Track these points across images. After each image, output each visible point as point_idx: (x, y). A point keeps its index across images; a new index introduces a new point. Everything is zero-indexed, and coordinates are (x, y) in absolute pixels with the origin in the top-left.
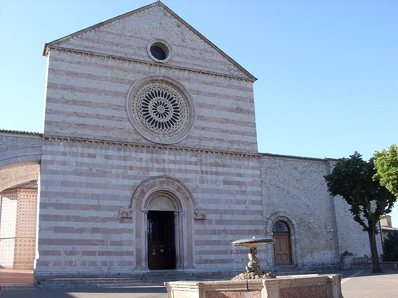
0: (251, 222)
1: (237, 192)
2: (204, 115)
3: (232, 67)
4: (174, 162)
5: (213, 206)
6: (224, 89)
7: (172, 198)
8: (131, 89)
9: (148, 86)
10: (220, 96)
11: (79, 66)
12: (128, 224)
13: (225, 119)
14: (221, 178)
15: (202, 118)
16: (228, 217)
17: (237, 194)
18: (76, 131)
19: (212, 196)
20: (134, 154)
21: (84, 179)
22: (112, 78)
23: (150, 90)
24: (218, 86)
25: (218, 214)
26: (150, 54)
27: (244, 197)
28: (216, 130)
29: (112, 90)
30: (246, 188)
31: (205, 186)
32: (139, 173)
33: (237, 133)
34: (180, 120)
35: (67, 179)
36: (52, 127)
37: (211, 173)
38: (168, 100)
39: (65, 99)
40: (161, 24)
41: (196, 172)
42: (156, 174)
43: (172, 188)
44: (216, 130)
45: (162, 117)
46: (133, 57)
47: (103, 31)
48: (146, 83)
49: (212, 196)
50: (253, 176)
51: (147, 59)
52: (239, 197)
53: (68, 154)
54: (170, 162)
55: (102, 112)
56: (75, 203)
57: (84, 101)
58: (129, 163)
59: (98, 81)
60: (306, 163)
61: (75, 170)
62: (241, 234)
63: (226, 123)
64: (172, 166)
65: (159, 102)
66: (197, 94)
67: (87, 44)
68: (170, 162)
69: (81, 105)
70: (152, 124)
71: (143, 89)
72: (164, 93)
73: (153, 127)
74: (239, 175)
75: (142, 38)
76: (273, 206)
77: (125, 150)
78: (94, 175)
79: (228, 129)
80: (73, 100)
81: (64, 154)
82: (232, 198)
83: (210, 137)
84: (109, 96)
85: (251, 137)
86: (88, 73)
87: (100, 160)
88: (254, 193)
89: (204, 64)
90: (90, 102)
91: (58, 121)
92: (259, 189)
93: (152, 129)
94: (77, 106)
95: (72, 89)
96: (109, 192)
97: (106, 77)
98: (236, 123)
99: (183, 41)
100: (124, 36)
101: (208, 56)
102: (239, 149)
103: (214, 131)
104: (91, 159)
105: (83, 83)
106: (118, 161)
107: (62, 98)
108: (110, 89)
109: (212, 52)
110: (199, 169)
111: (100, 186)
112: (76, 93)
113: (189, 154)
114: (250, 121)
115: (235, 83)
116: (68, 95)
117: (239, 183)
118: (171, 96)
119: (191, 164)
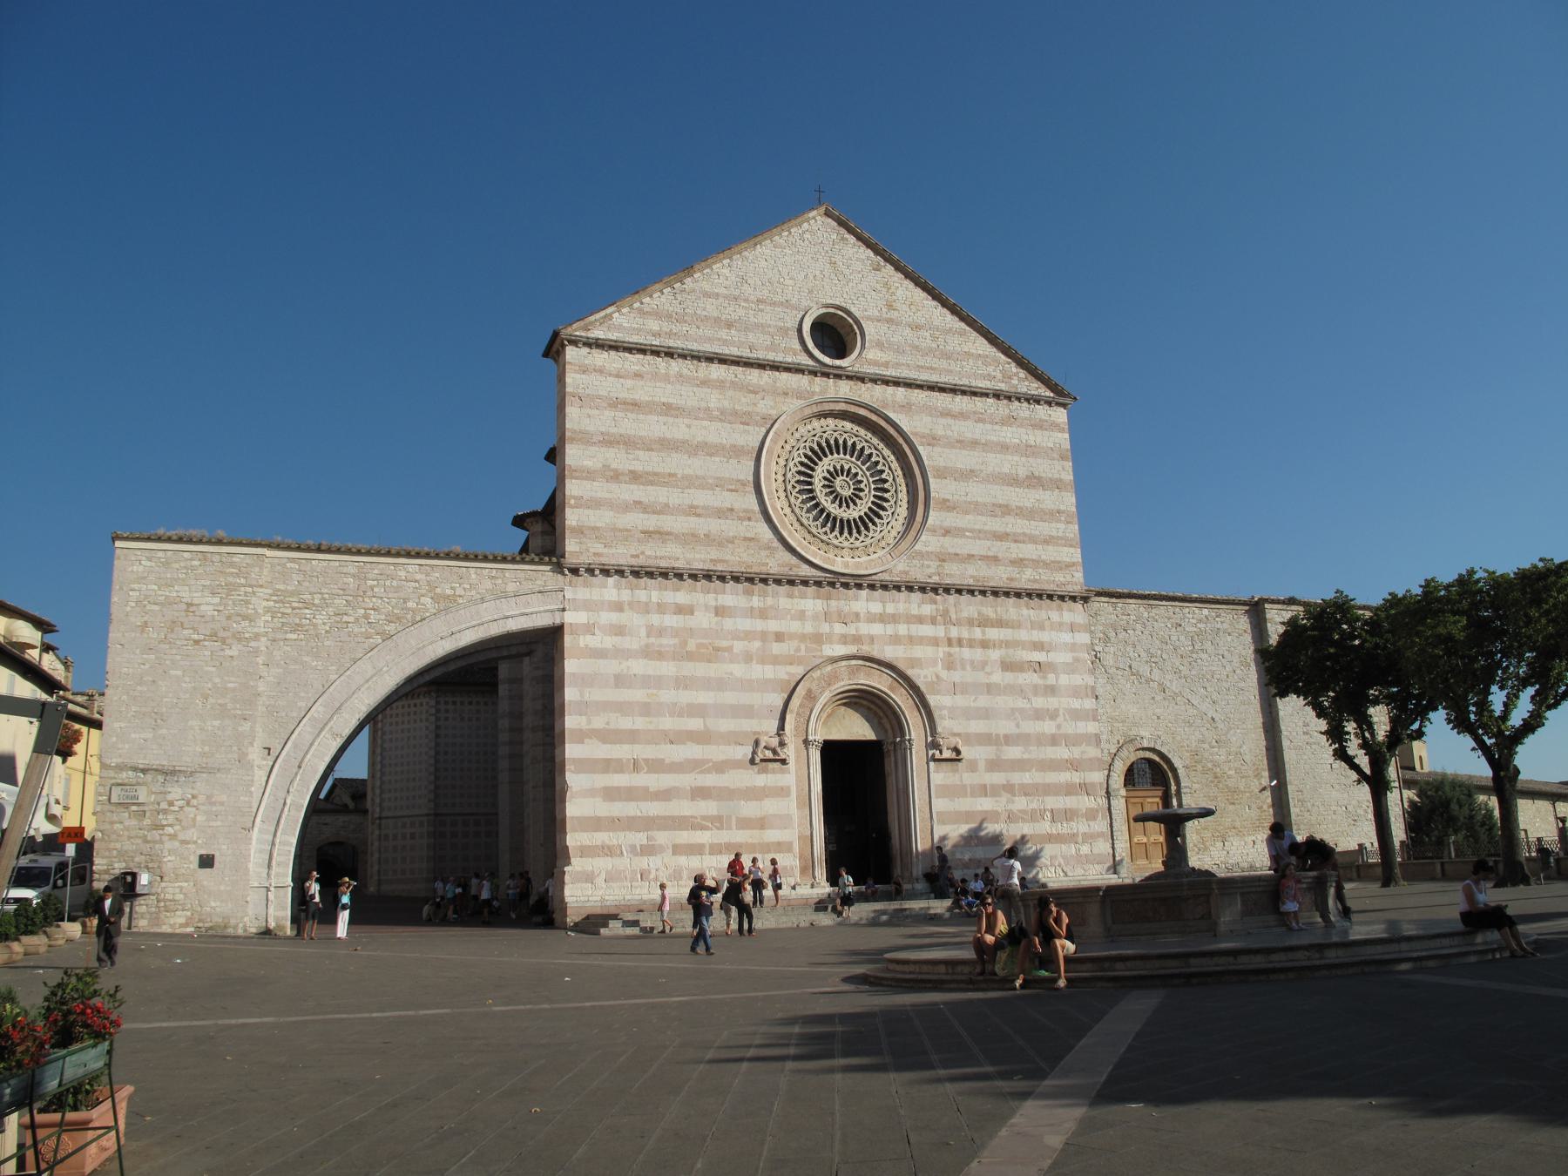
0: (1074, 765)
1: (1036, 689)
2: (949, 497)
3: (1014, 370)
4: (882, 618)
5: (977, 727)
6: (997, 427)
7: (878, 711)
9: (809, 427)
10: (987, 446)
11: (642, 383)
12: (779, 776)
13: (1000, 506)
14: (995, 655)
15: (947, 506)
16: (1013, 752)
17: (1036, 694)
18: (642, 548)
19: (974, 701)
20: (784, 602)
21: (667, 668)
22: (722, 412)
23: (816, 439)
24: (980, 420)
25: (991, 745)
27: (1052, 703)
28: (979, 534)
29: (725, 441)
30: (1057, 681)
31: (957, 676)
32: (798, 650)
33: (1032, 539)
34: (890, 512)
35: (628, 668)
36: (584, 540)
37: (971, 644)
38: (859, 463)
39: (612, 470)
41: (935, 642)
42: (841, 650)
43: (879, 683)
44: (979, 534)
45: (848, 507)
46: (771, 356)
49: (976, 699)
50: (1073, 647)
51: (805, 361)
52: (1039, 702)
53: (626, 607)
54: (872, 618)
55: (702, 498)
56: (651, 727)
57: (656, 474)
58: (773, 626)
59: (686, 421)
60: (1206, 612)
61: (647, 646)
62: (1049, 795)
63: (1004, 514)
64: (877, 629)
65: (839, 468)
66: (929, 445)
67: (654, 325)
68: (872, 618)
69: (652, 483)
70: (823, 526)
71: (797, 435)
72: (849, 443)
73: (826, 533)
74: (1039, 646)
75: (786, 304)
76: (1123, 722)
77: (764, 595)
78: (690, 657)
79: (1008, 530)
80: (631, 472)
81: (618, 607)
82: (1021, 703)
83: (964, 551)
84: (717, 459)
85: (1066, 549)
86: (663, 400)
87: (703, 620)
88: (1076, 692)
89: (943, 364)
90: (670, 475)
91: (598, 525)
92: (1090, 680)
93: (824, 538)
94: (641, 487)
95: (628, 443)
96: (730, 698)
97: (708, 409)
98: (1030, 514)
99: (890, 306)
100: (746, 300)
102: (1035, 581)
103: (974, 538)
104: (681, 617)
105: (654, 427)
106: (749, 620)
107: (604, 466)
108: (720, 441)
110: (943, 635)
111: (707, 684)
112: (637, 452)
113: (917, 596)
114: (1062, 508)
115: (1022, 410)
116: (618, 459)
118: (867, 452)
119: (921, 623)
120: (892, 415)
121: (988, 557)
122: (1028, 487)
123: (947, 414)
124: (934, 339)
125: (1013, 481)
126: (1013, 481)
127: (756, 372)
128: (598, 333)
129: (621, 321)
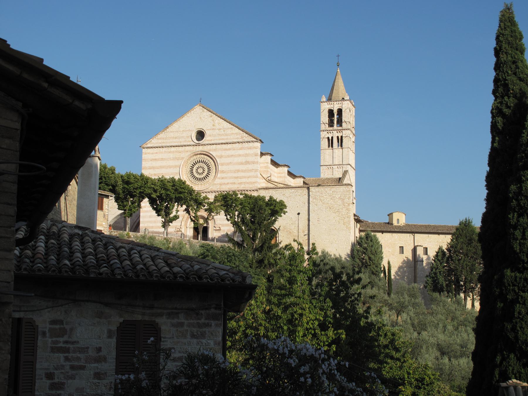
6: (238, 151)
8: (183, 162)
9: (193, 158)
13: (237, 170)
15: (223, 172)
24: (234, 150)
28: (231, 178)
33: (245, 177)
40: (201, 118)
44: (231, 178)
47: (169, 131)
48: (191, 157)
67: (160, 141)
83: (227, 182)
89: (226, 137)
93: (195, 183)
97: (170, 158)
100: (180, 131)
101: (229, 132)
109: (231, 128)
114: (254, 168)
115: (246, 145)
120: (211, 153)
121: (232, 183)
122: (245, 164)
123: (226, 150)
124: (224, 131)
125: (242, 163)
126: (242, 163)
127: (181, 147)
128: (149, 145)
129: (154, 142)
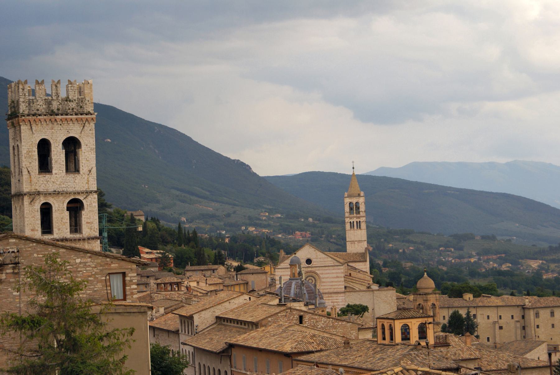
10: (331, 273)
14: (330, 301)
26: (305, 263)
33: (337, 285)
37: (327, 300)
50: (342, 299)
67: (285, 265)
74: (337, 299)
89: (324, 263)
99: (317, 256)
101: (326, 260)
109: (327, 258)
115: (336, 267)
117: (336, 302)
120: (316, 271)
123: (325, 270)
126: (335, 278)
